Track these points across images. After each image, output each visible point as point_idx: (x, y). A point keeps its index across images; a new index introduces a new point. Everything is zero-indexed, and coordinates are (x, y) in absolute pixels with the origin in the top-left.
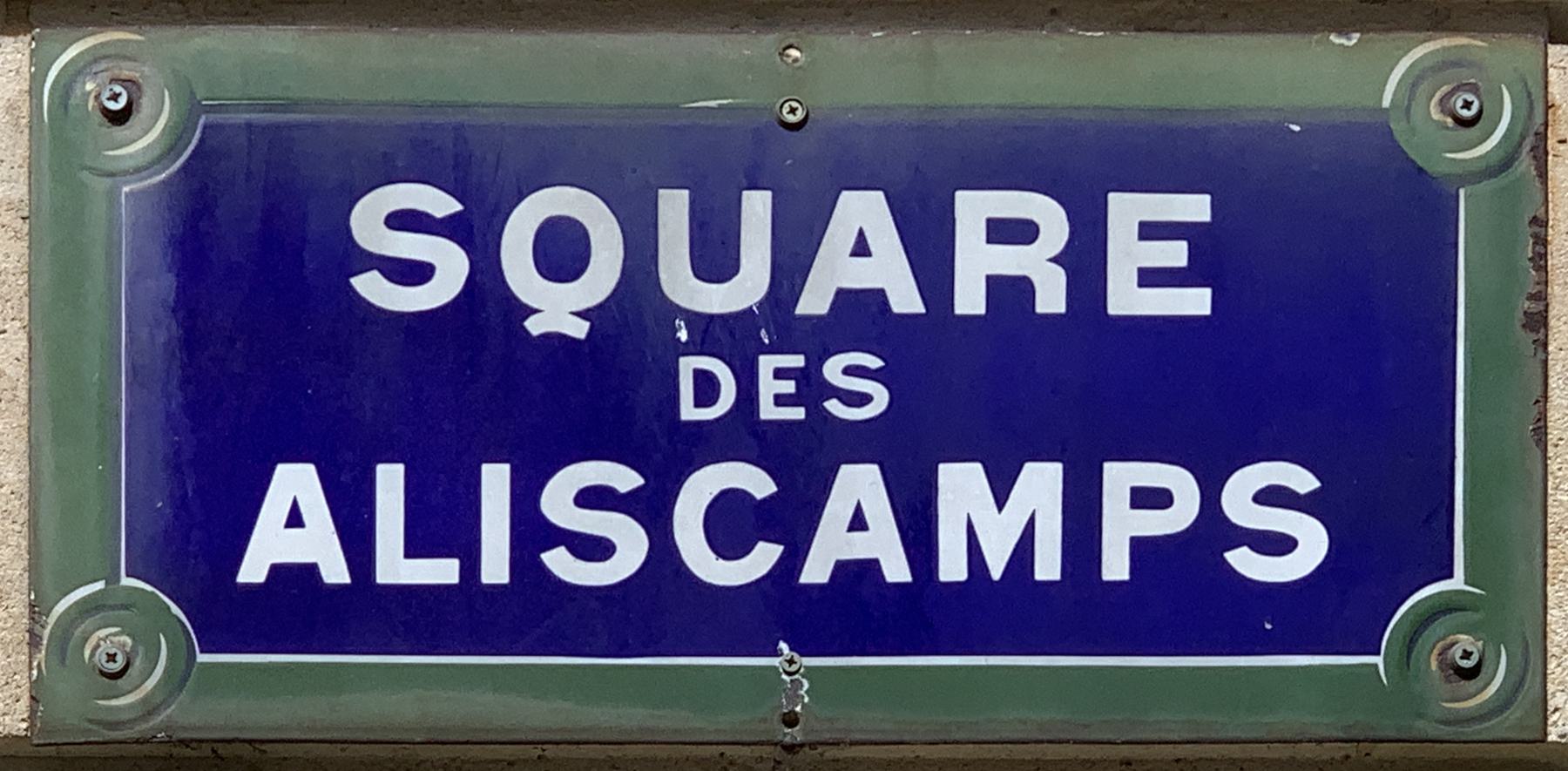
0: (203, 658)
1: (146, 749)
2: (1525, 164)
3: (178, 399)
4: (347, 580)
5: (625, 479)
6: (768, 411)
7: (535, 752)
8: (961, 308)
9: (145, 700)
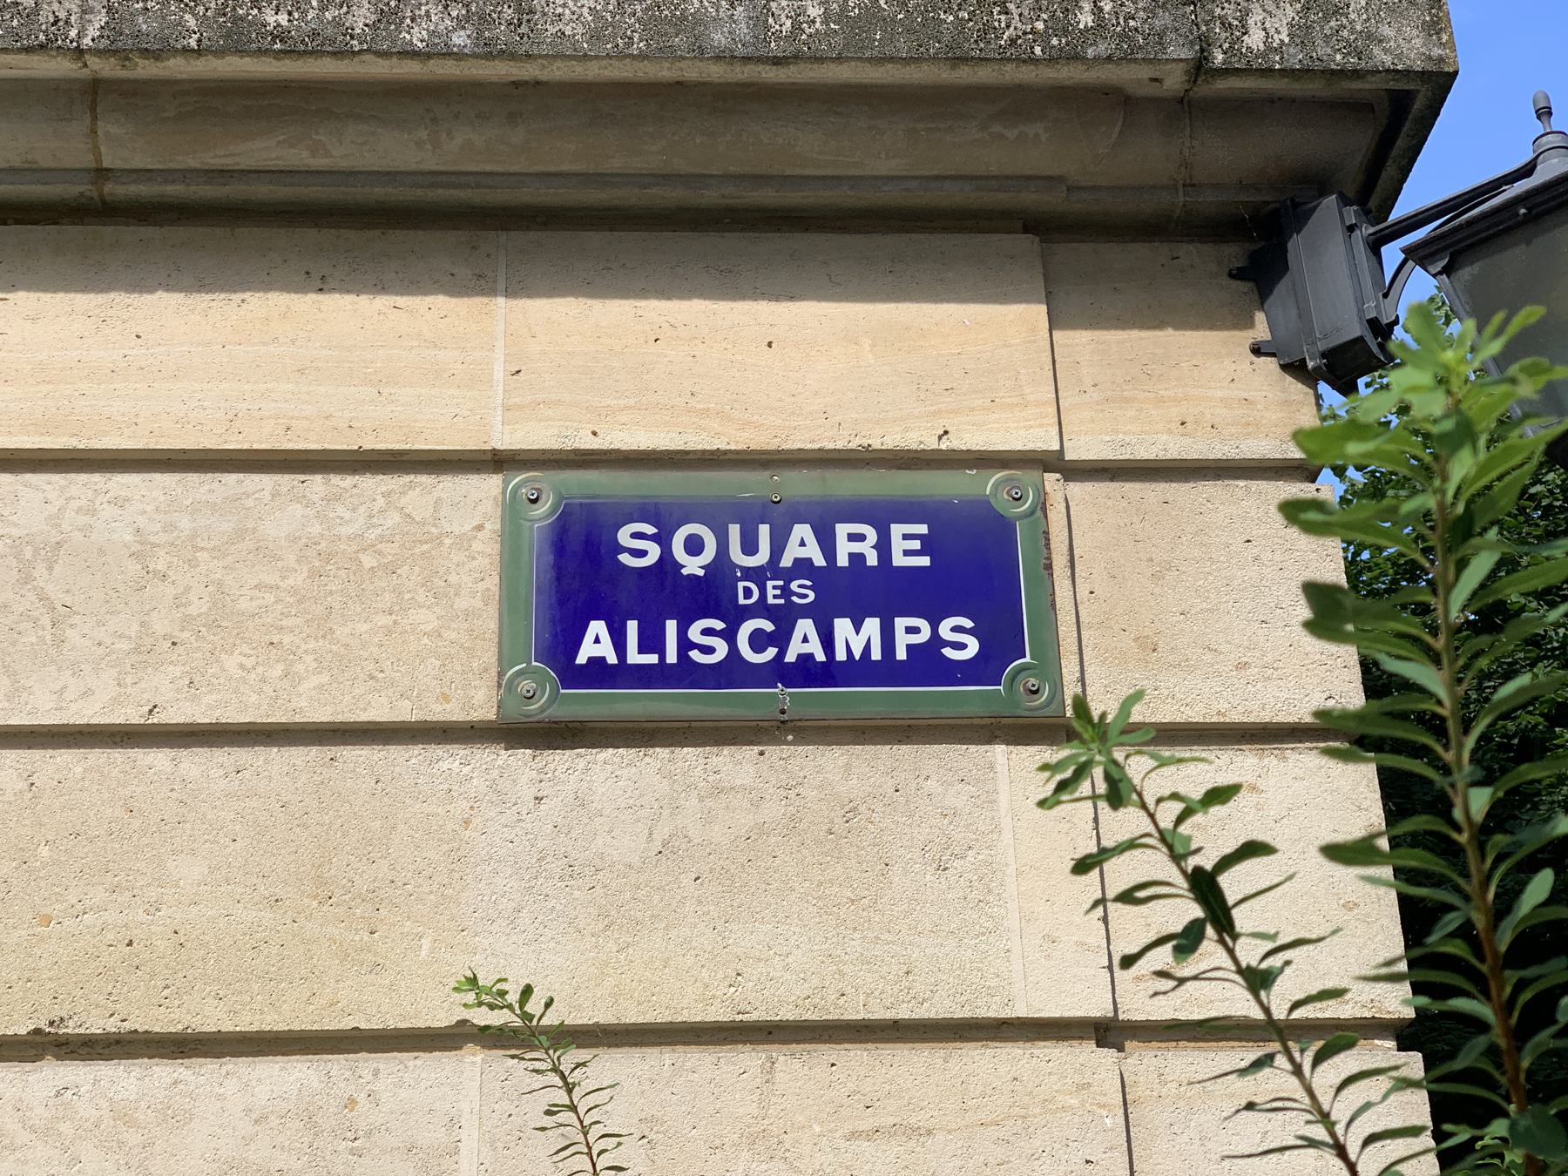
0: (562, 691)
1: (541, 725)
2: (1039, 513)
3: (554, 600)
4: (616, 662)
5: (719, 625)
6: (771, 600)
7: (687, 725)
8: (840, 564)
9: (541, 706)
